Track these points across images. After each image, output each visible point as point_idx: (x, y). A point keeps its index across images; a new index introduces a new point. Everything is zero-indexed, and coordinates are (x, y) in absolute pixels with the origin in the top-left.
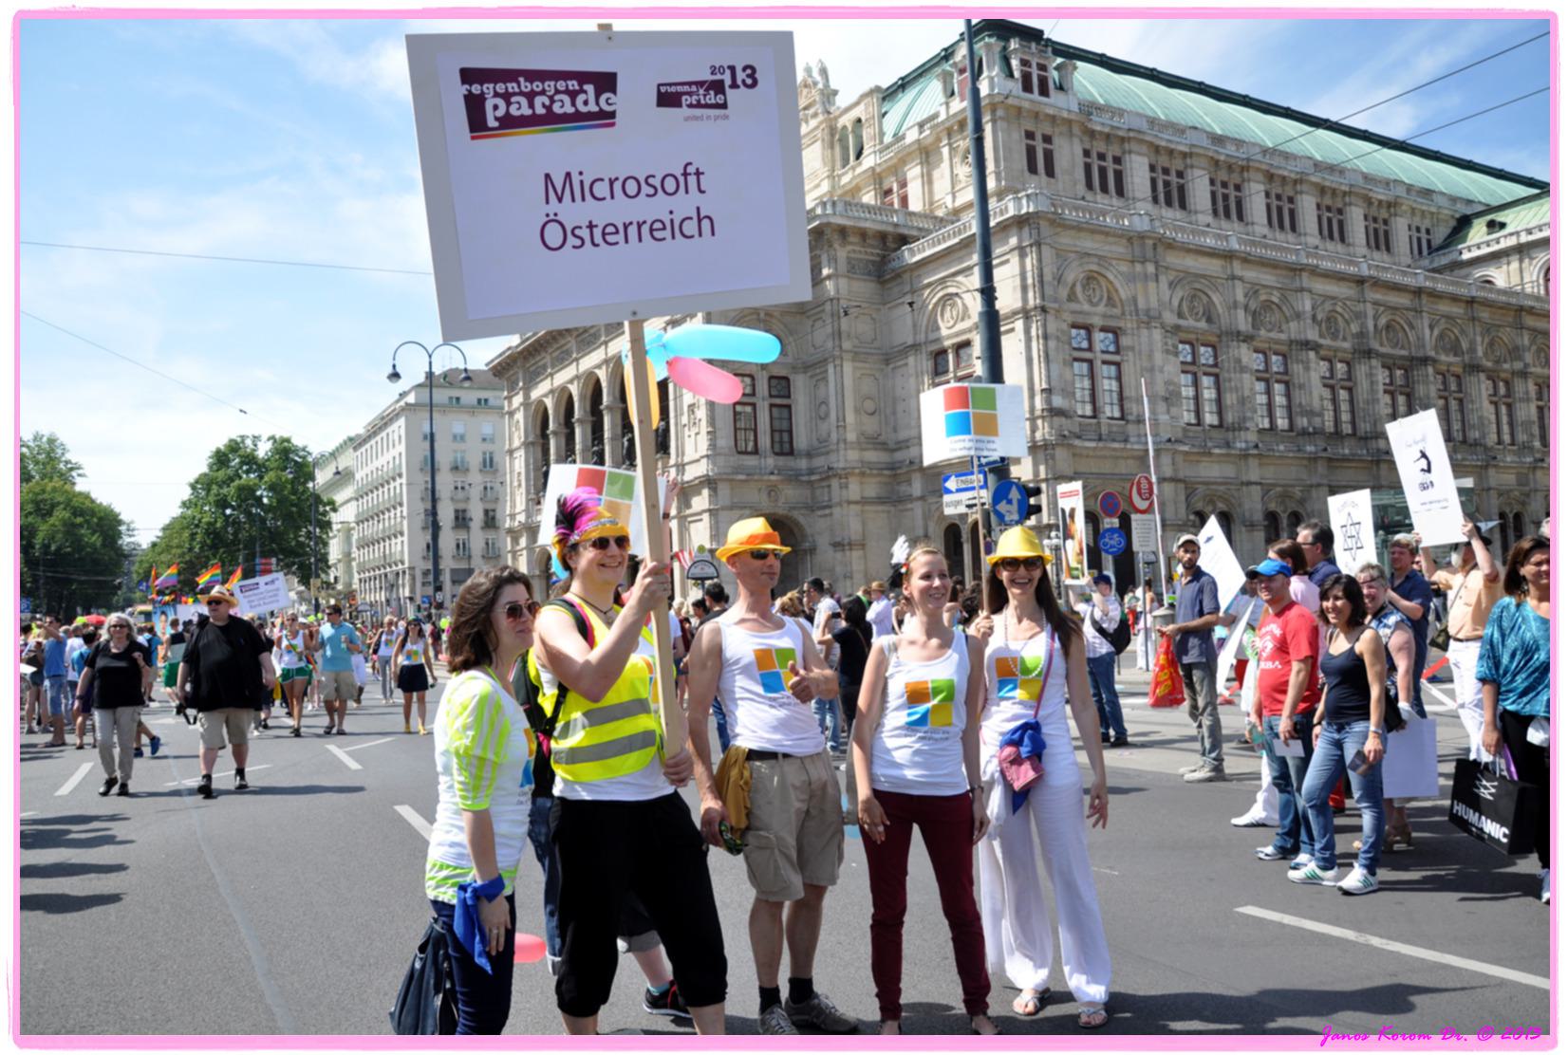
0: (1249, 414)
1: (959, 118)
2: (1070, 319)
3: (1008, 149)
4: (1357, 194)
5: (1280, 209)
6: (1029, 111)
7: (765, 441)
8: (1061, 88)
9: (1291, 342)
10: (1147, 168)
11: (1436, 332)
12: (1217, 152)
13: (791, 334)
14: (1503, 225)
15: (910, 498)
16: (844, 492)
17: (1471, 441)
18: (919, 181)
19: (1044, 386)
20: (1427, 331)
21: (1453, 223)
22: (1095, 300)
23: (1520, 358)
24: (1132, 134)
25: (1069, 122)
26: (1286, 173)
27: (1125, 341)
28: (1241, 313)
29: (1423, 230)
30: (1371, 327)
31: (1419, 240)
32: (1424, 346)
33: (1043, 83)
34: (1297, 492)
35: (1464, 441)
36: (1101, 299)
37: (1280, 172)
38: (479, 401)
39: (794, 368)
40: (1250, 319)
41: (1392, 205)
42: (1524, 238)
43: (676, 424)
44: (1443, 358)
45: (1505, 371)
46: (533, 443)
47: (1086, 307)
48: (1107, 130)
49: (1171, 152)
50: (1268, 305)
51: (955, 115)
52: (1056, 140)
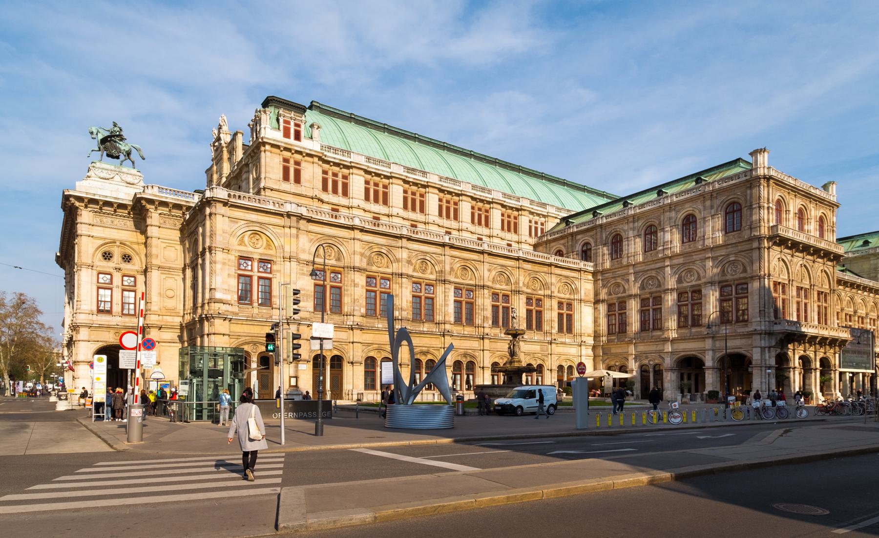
0: (356, 308)
5: (448, 209)
11: (494, 273)
12: (407, 177)
20: (486, 274)
24: (353, 164)
28: (357, 258)
29: (539, 223)
30: (448, 268)
31: (536, 228)
36: (262, 246)
37: (448, 189)
40: (365, 260)
44: (498, 286)
50: (380, 254)
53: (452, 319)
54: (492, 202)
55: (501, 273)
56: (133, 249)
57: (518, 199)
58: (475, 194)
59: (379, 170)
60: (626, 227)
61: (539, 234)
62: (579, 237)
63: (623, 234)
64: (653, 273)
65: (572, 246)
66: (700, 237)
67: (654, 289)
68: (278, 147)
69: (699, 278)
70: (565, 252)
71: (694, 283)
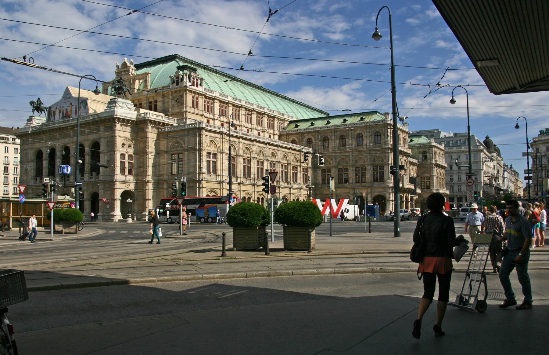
1: (176, 90)
2: (207, 151)
6: (194, 91)
7: (127, 171)
8: (201, 85)
15: (163, 188)
18: (161, 102)
21: (288, 122)
25: (202, 95)
33: (197, 83)
41: (274, 117)
42: (303, 131)
44: (283, 162)
47: (210, 149)
48: (210, 96)
49: (224, 102)
50: (247, 148)
54: (264, 114)
55: (284, 155)
58: (259, 110)
60: (331, 134)
61: (281, 130)
62: (306, 135)
63: (329, 137)
64: (344, 157)
65: (302, 139)
66: (365, 144)
67: (344, 164)
69: (364, 162)
70: (297, 141)
71: (362, 164)
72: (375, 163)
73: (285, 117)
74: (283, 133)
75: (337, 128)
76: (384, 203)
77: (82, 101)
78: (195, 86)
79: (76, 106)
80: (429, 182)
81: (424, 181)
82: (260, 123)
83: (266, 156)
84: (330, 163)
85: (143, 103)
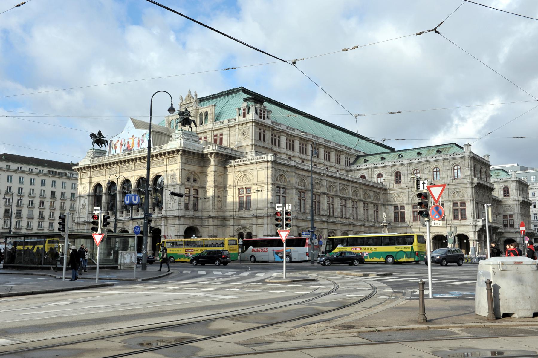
1: (242, 122)
2: (276, 186)
3: (255, 133)
4: (333, 149)
7: (191, 207)
9: (321, 193)
10: (286, 140)
11: (352, 191)
13: (199, 178)
14: (368, 161)
16: (213, 222)
17: (359, 219)
19: (271, 202)
20: (351, 191)
21: (355, 157)
22: (282, 181)
23: (370, 198)
24: (283, 131)
25: (269, 127)
26: (317, 142)
27: (287, 191)
29: (348, 159)
30: (339, 190)
31: (347, 161)
32: (349, 195)
34: (320, 229)
35: (357, 219)
38: (18, 168)
39: (199, 187)
41: (341, 151)
42: (373, 166)
43: (165, 200)
44: (354, 198)
45: (367, 202)
46: (92, 195)
48: (277, 129)
49: (291, 135)
50: (317, 183)
51: (241, 121)
52: (266, 131)
53: (340, 215)
54: (332, 148)
55: (354, 191)
56: (198, 176)
57: (341, 146)
58: (326, 144)
59: (292, 133)
60: (403, 169)
62: (375, 170)
63: (401, 172)
68: (258, 123)
70: (366, 177)
72: (453, 199)
73: (353, 151)
74: (351, 169)
75: (410, 162)
76: (493, 243)
77: (145, 133)
78: (262, 118)
79: (139, 138)
80: (512, 221)
81: (507, 220)
82: (327, 158)
83: (336, 191)
84: (403, 199)
85: (208, 136)
